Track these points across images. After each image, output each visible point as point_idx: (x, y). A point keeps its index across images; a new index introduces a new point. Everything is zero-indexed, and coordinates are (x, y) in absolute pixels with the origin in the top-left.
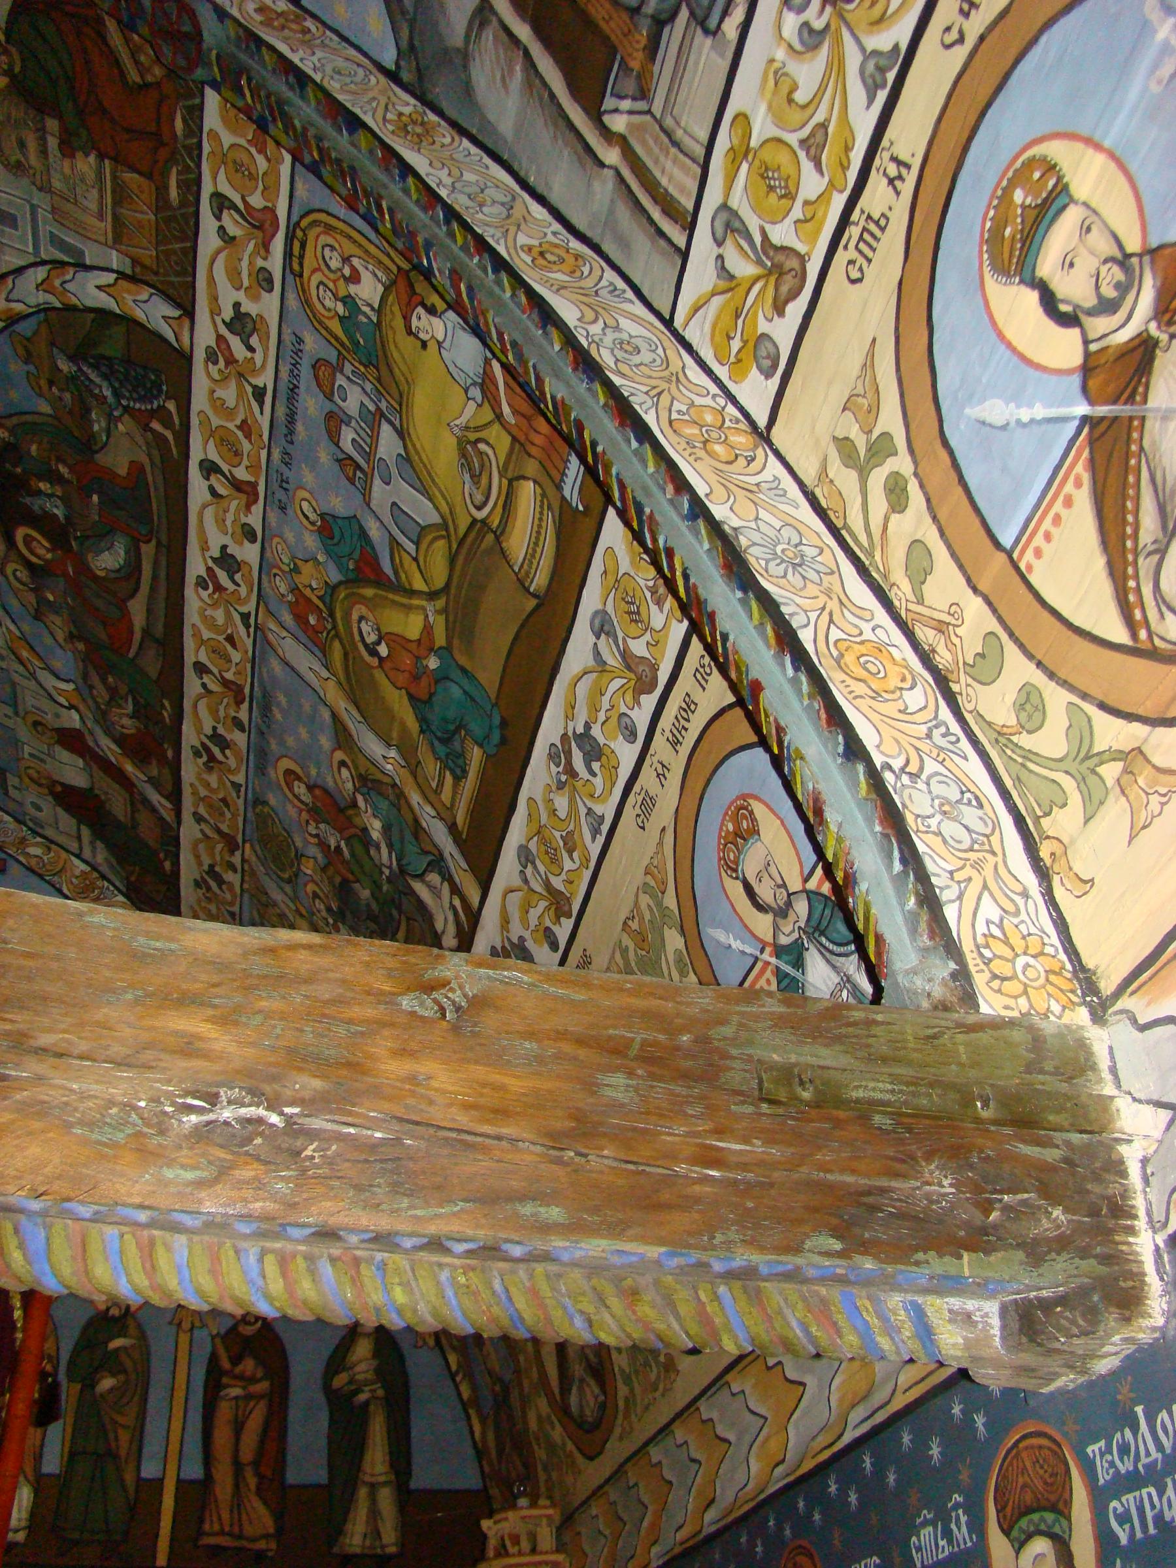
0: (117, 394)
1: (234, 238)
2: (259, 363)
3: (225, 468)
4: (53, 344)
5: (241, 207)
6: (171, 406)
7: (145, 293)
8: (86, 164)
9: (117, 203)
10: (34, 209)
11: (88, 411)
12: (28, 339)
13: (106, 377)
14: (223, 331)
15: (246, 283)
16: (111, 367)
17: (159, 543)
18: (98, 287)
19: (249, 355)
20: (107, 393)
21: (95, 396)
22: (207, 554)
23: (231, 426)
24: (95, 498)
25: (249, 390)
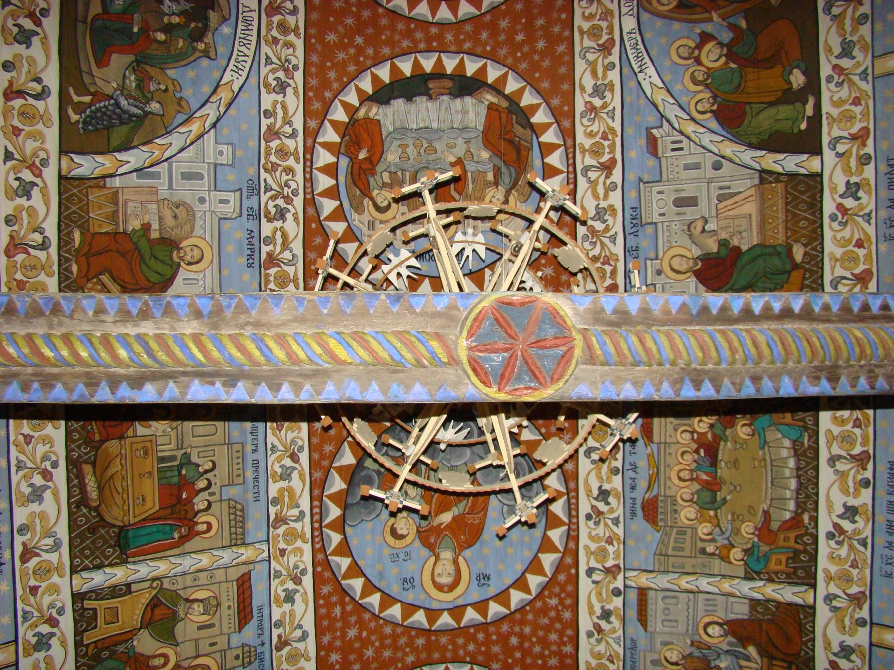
0: (117, 105)
1: (34, 232)
2: (12, 173)
3: (31, 101)
4: (163, 115)
5: (30, 250)
6: (74, 117)
7: (97, 173)
8: (135, 224)
9: (117, 211)
10: (170, 187)
11: (138, 86)
12: (179, 112)
13: (125, 112)
14: (38, 180)
15: (24, 213)
16: (120, 117)
17: (85, 21)
18: (128, 162)
19: (19, 175)
20: (123, 102)
21: (131, 97)
22: (42, 35)
23: (27, 128)
24: (135, 30)
25: (17, 156)
